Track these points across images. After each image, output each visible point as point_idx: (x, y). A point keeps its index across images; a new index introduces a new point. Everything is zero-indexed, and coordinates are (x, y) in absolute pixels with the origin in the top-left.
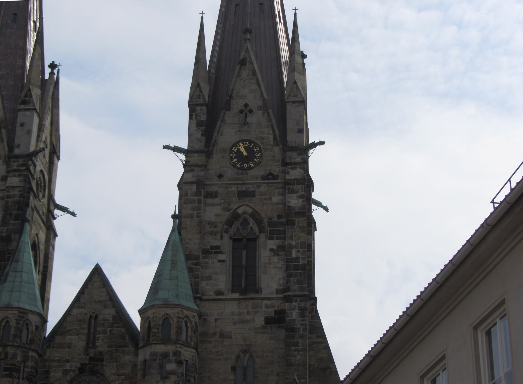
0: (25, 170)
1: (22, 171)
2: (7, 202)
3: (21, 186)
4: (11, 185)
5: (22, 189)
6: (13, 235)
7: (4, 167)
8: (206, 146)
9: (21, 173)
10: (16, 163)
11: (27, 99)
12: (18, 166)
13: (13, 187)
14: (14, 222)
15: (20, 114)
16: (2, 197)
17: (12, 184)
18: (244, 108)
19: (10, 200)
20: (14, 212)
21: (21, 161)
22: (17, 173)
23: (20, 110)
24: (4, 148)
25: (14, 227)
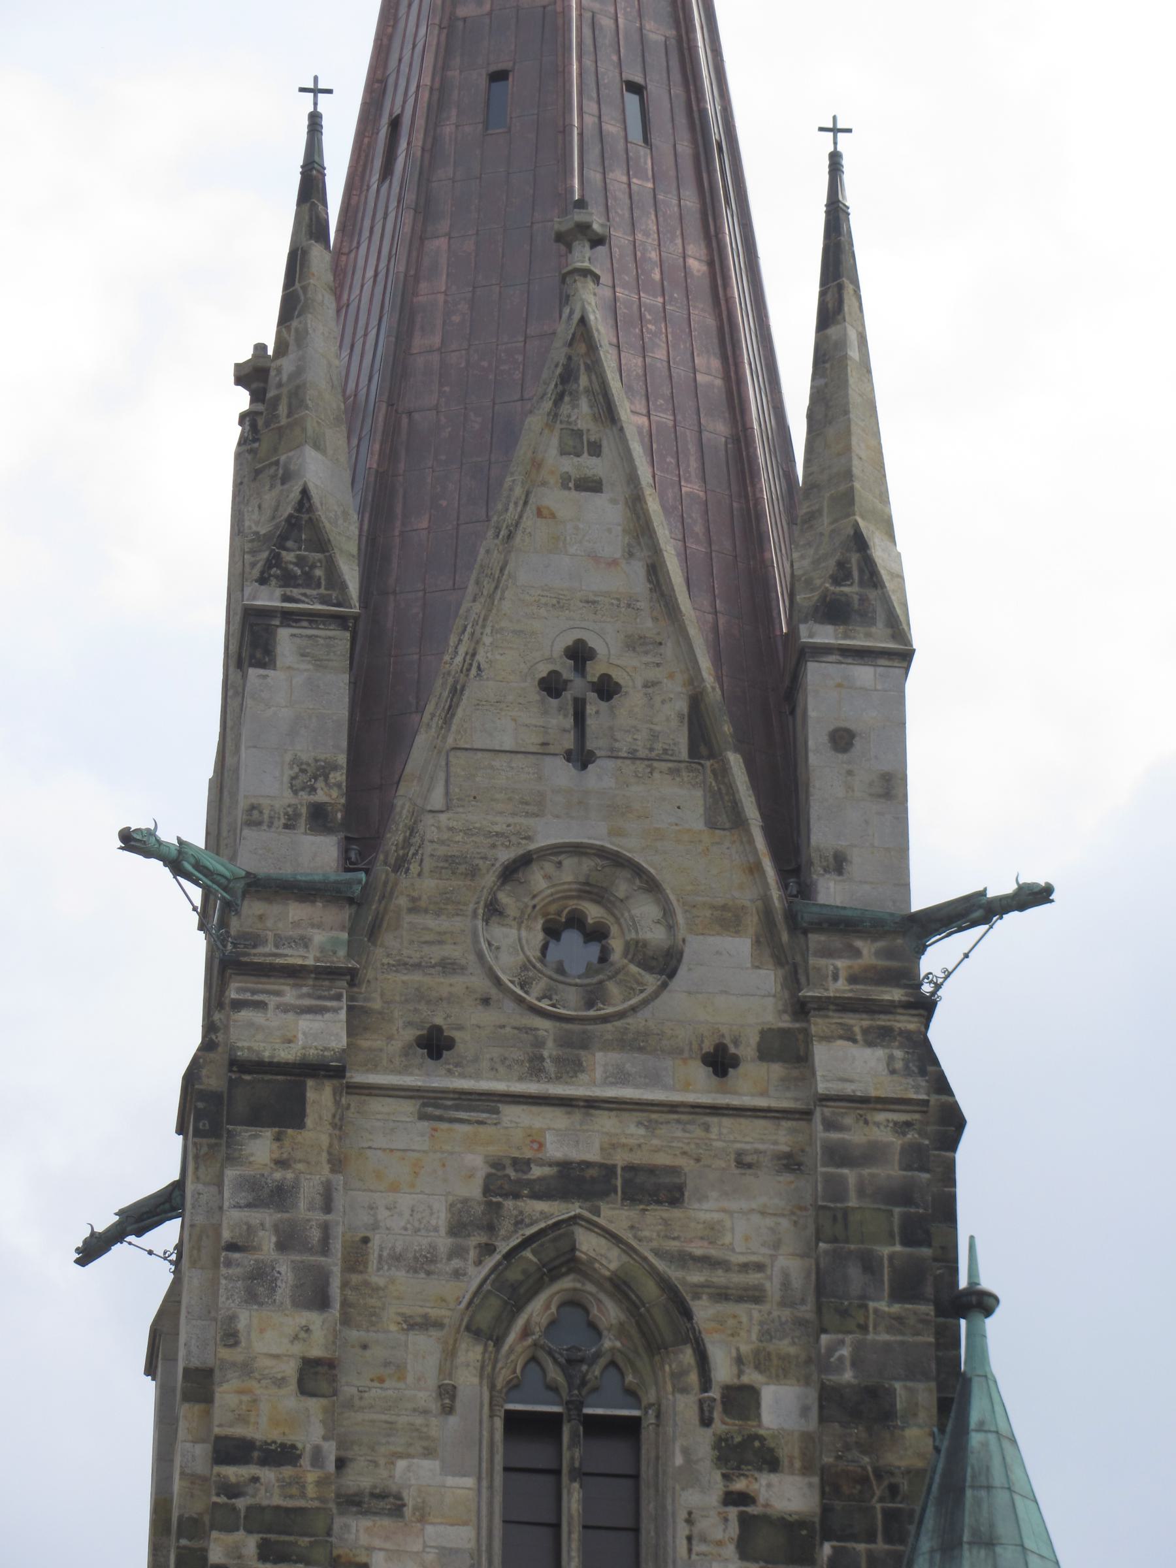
0: (907, 1006)
1: (888, 1008)
2: (835, 1189)
3: (912, 1095)
4: (849, 1089)
5: (917, 1116)
6: (898, 1385)
7: (769, 979)
8: (348, 865)
9: (883, 1021)
10: (840, 963)
11: (846, 589)
12: (853, 979)
13: (865, 1100)
14: (896, 1308)
15: (815, 673)
16: (788, 1156)
17: (851, 1081)
18: (566, 669)
19: (850, 1175)
20: (885, 1251)
21: (868, 952)
22: (858, 1023)
23: (821, 651)
24: (755, 869)
25: (899, 1338)
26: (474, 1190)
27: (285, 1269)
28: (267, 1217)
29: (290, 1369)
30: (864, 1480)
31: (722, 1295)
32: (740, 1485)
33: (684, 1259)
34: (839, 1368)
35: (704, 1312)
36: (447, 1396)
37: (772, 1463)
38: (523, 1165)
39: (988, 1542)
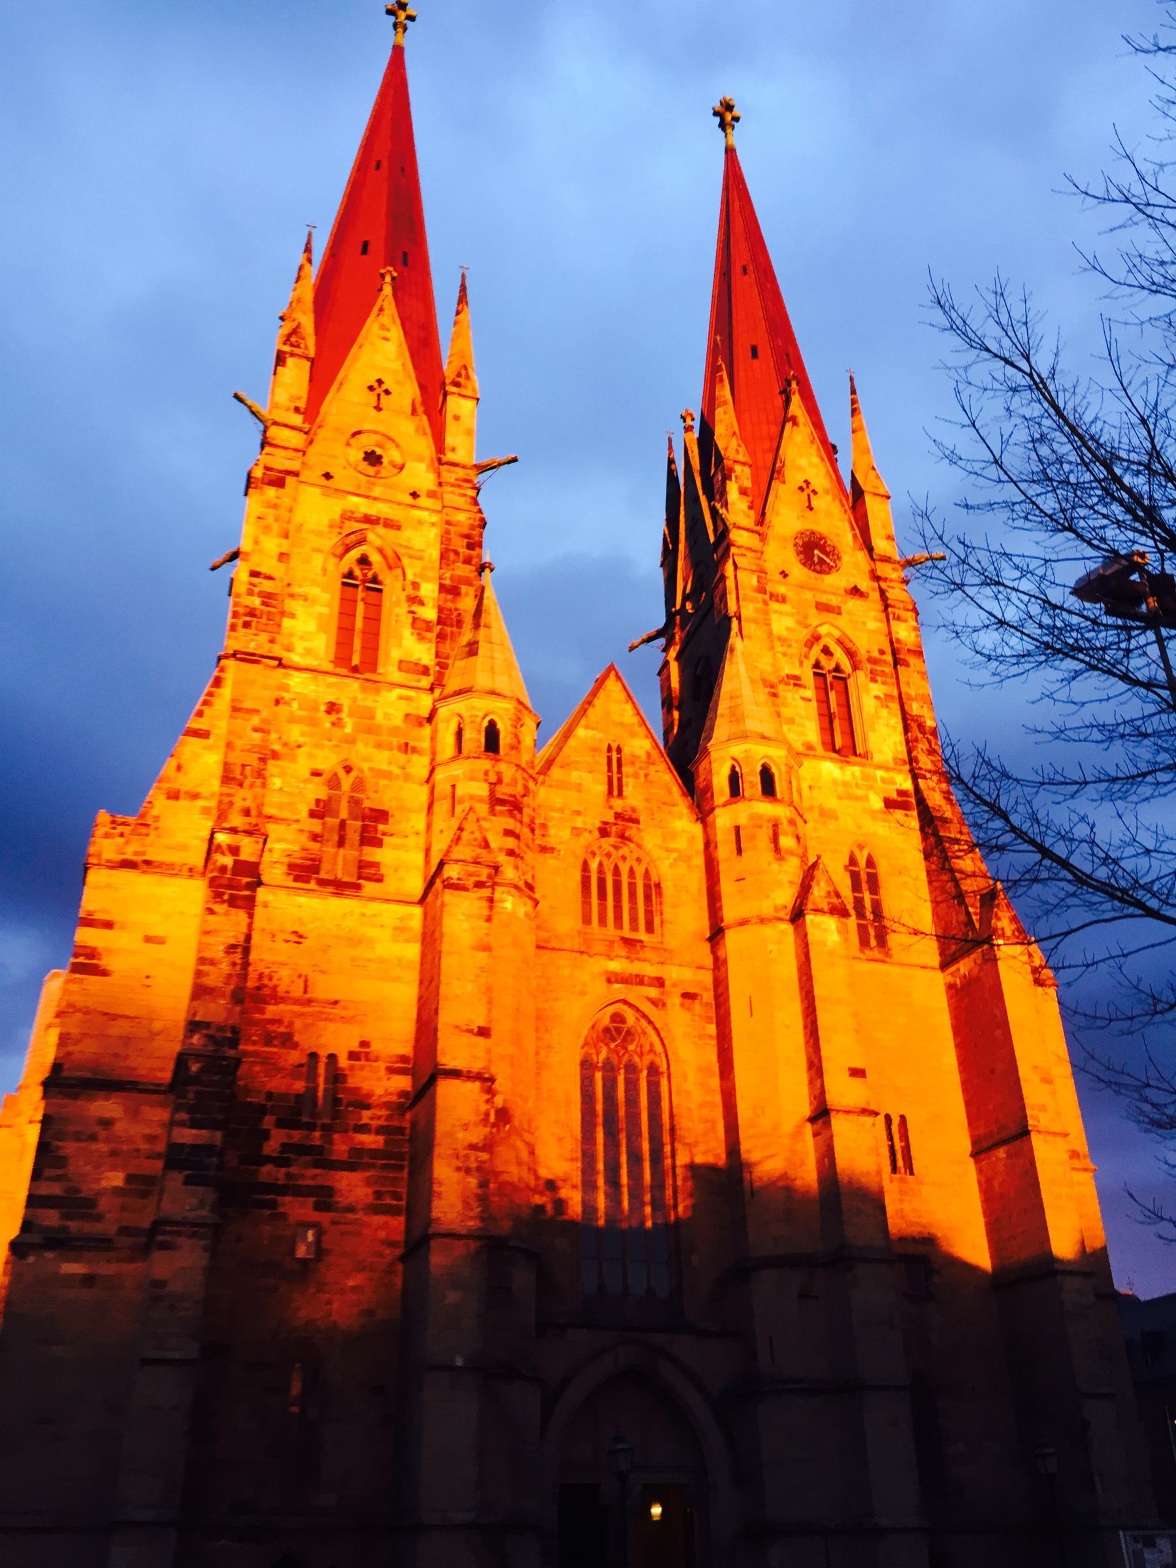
19: (452, 529)
26: (337, 517)
27: (276, 526)
28: (271, 511)
29: (275, 554)
30: (450, 610)
31: (411, 557)
32: (413, 608)
33: (400, 545)
34: (445, 579)
35: (405, 561)
36: (325, 570)
37: (422, 603)
38: (353, 512)
39: (488, 627)
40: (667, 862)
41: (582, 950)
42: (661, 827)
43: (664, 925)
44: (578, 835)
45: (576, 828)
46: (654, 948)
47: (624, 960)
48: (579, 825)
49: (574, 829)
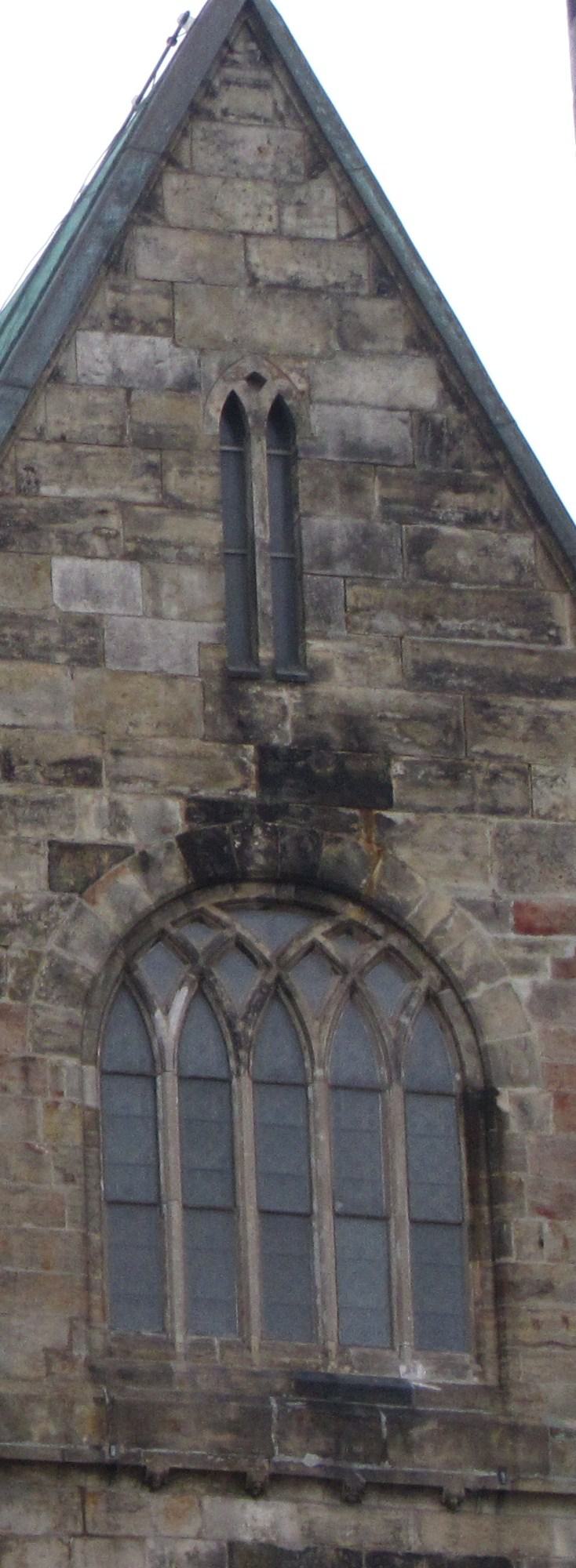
40: (523, 985)
41: (114, 1452)
42: (494, 811)
43: (510, 1303)
44: (85, 886)
45: (76, 849)
46: (458, 1427)
47: (316, 1495)
48: (91, 831)
49: (60, 851)
